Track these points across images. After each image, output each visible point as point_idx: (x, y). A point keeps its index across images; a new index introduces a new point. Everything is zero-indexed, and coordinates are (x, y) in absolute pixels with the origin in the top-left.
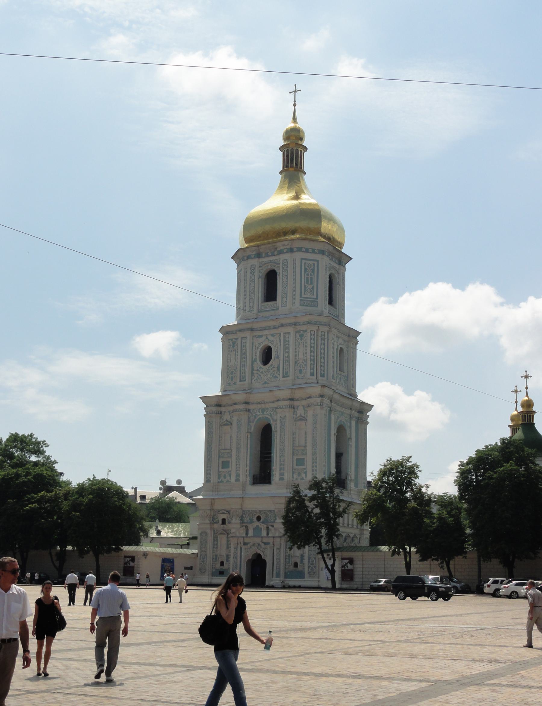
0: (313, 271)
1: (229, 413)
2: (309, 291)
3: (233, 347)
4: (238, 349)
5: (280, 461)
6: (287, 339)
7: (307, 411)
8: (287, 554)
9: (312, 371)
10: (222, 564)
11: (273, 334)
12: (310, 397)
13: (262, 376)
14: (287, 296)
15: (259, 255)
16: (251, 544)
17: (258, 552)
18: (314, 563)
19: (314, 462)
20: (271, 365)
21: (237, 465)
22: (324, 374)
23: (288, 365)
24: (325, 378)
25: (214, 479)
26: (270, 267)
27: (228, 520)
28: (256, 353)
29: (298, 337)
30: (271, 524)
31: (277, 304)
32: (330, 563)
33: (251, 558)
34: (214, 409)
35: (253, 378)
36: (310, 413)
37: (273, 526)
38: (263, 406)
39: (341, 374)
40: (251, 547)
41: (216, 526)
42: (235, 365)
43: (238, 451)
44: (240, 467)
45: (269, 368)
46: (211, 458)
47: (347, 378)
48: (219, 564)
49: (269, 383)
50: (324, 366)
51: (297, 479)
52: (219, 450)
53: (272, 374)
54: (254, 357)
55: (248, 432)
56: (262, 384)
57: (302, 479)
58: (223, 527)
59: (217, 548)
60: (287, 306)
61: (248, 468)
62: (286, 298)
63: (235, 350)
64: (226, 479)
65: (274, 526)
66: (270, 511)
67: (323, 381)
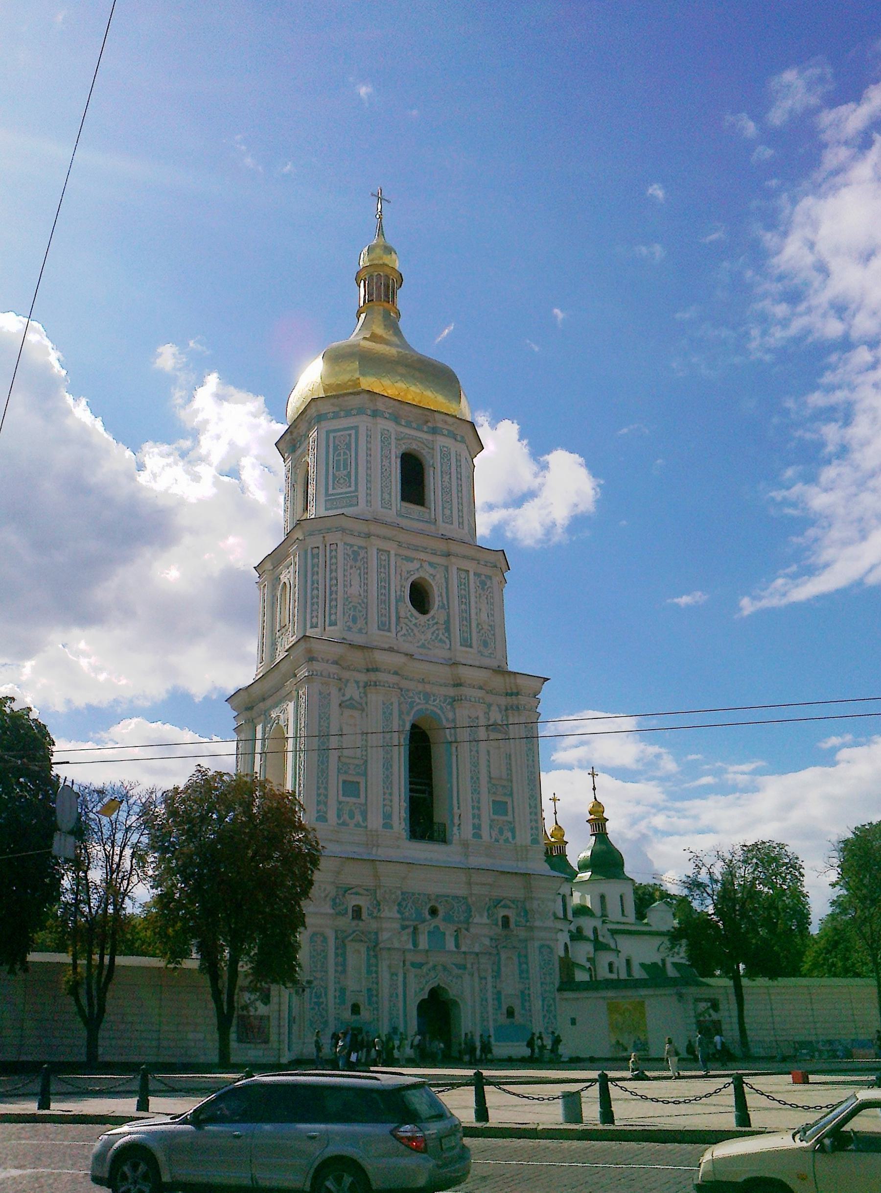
1: (355, 685)
3: (355, 560)
10: (356, 1009)
12: (517, 694)
13: (416, 631)
14: (452, 507)
15: (396, 419)
17: (441, 985)
18: (553, 1008)
20: (433, 618)
21: (384, 794)
26: (414, 446)
27: (368, 908)
33: (426, 997)
35: (399, 631)
37: (467, 930)
38: (428, 688)
40: (427, 974)
42: (360, 595)
44: (391, 801)
45: (428, 620)
46: (327, 769)
49: (430, 649)
53: (435, 635)
54: (398, 593)
57: (507, 840)
58: (357, 925)
59: (344, 971)
60: (452, 524)
62: (451, 509)
63: (360, 568)
65: (472, 930)
66: (456, 897)
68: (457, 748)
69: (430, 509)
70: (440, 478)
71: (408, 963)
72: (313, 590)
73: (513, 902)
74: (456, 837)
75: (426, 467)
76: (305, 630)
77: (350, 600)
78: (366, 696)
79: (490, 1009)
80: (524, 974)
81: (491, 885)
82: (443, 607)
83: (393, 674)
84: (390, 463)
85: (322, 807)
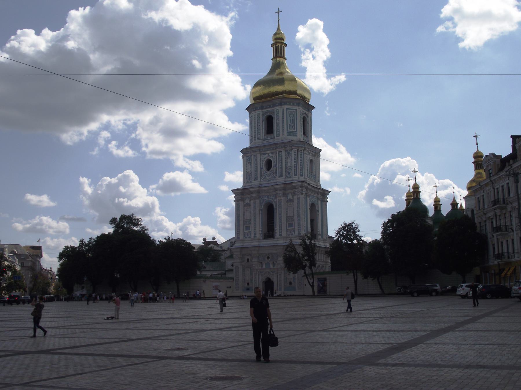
0: (294, 115)
1: (248, 199)
2: (292, 127)
3: (249, 161)
4: (252, 162)
5: (279, 225)
6: (280, 155)
7: (293, 196)
9: (295, 173)
10: (248, 284)
11: (272, 153)
15: (262, 108)
19: (299, 224)
20: (272, 171)
21: (254, 228)
22: (302, 174)
24: (303, 177)
25: (242, 237)
26: (268, 114)
28: (263, 164)
29: (287, 154)
31: (273, 135)
32: (311, 281)
33: (264, 280)
36: (296, 197)
37: (276, 262)
39: (312, 174)
43: (255, 220)
44: (256, 229)
47: (315, 176)
48: (247, 284)
50: (302, 170)
51: (289, 235)
52: (244, 221)
54: (261, 166)
57: (292, 235)
60: (279, 136)
61: (261, 229)
62: (279, 131)
63: (251, 163)
64: (248, 236)
65: (278, 262)
67: (302, 179)
84: (260, 124)
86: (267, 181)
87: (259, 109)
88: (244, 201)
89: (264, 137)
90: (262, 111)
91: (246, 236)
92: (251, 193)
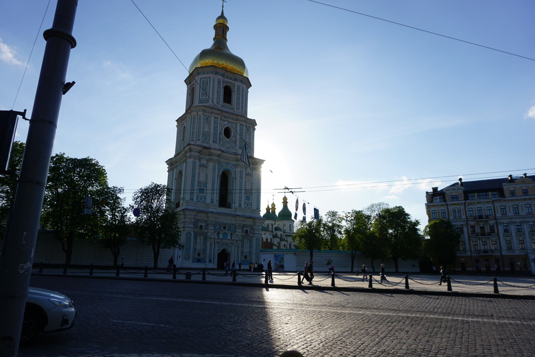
1: (205, 159)
3: (207, 120)
5: (239, 196)
6: (241, 128)
7: (252, 171)
8: (242, 251)
13: (225, 144)
16: (222, 243)
18: (259, 256)
20: (231, 140)
23: (241, 142)
26: (228, 84)
30: (234, 232)
31: (232, 107)
33: (220, 252)
34: (198, 154)
37: (235, 233)
38: (228, 161)
41: (195, 230)
42: (208, 131)
44: (214, 195)
46: (194, 185)
51: (246, 208)
52: (198, 181)
54: (220, 131)
55: (218, 175)
56: (226, 148)
57: (249, 208)
58: (201, 231)
59: (196, 244)
60: (239, 110)
61: (217, 196)
62: (239, 105)
63: (208, 123)
65: (236, 233)
66: (232, 224)
68: (236, 180)
69: (232, 105)
70: (236, 95)
71: (216, 242)
72: (193, 129)
73: (249, 226)
74: (233, 206)
75: (232, 91)
76: (190, 142)
77: (204, 133)
78: (208, 163)
79: (240, 255)
80: (251, 246)
81: (243, 221)
82: (234, 136)
83: (217, 157)
84: (220, 89)
85: (192, 196)
86: (226, 148)
87: (220, 75)
88: (200, 161)
89: (222, 103)
90: (223, 79)
91: (199, 199)
92: (211, 155)
